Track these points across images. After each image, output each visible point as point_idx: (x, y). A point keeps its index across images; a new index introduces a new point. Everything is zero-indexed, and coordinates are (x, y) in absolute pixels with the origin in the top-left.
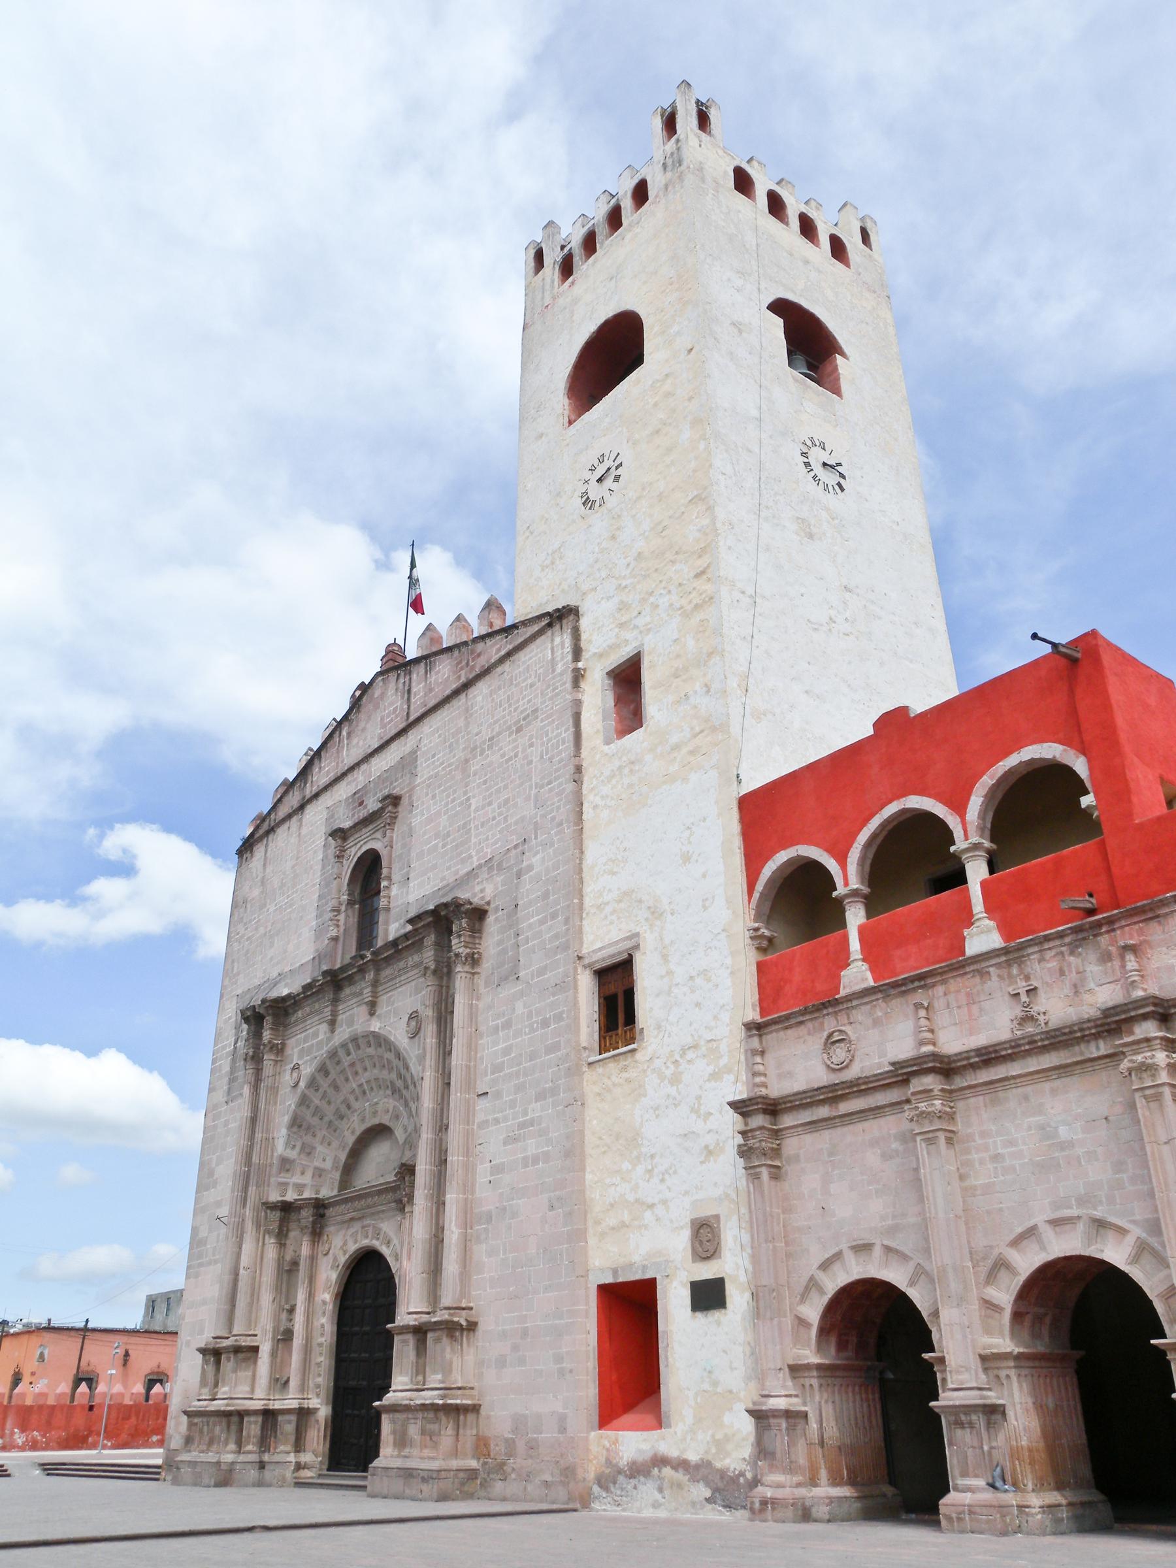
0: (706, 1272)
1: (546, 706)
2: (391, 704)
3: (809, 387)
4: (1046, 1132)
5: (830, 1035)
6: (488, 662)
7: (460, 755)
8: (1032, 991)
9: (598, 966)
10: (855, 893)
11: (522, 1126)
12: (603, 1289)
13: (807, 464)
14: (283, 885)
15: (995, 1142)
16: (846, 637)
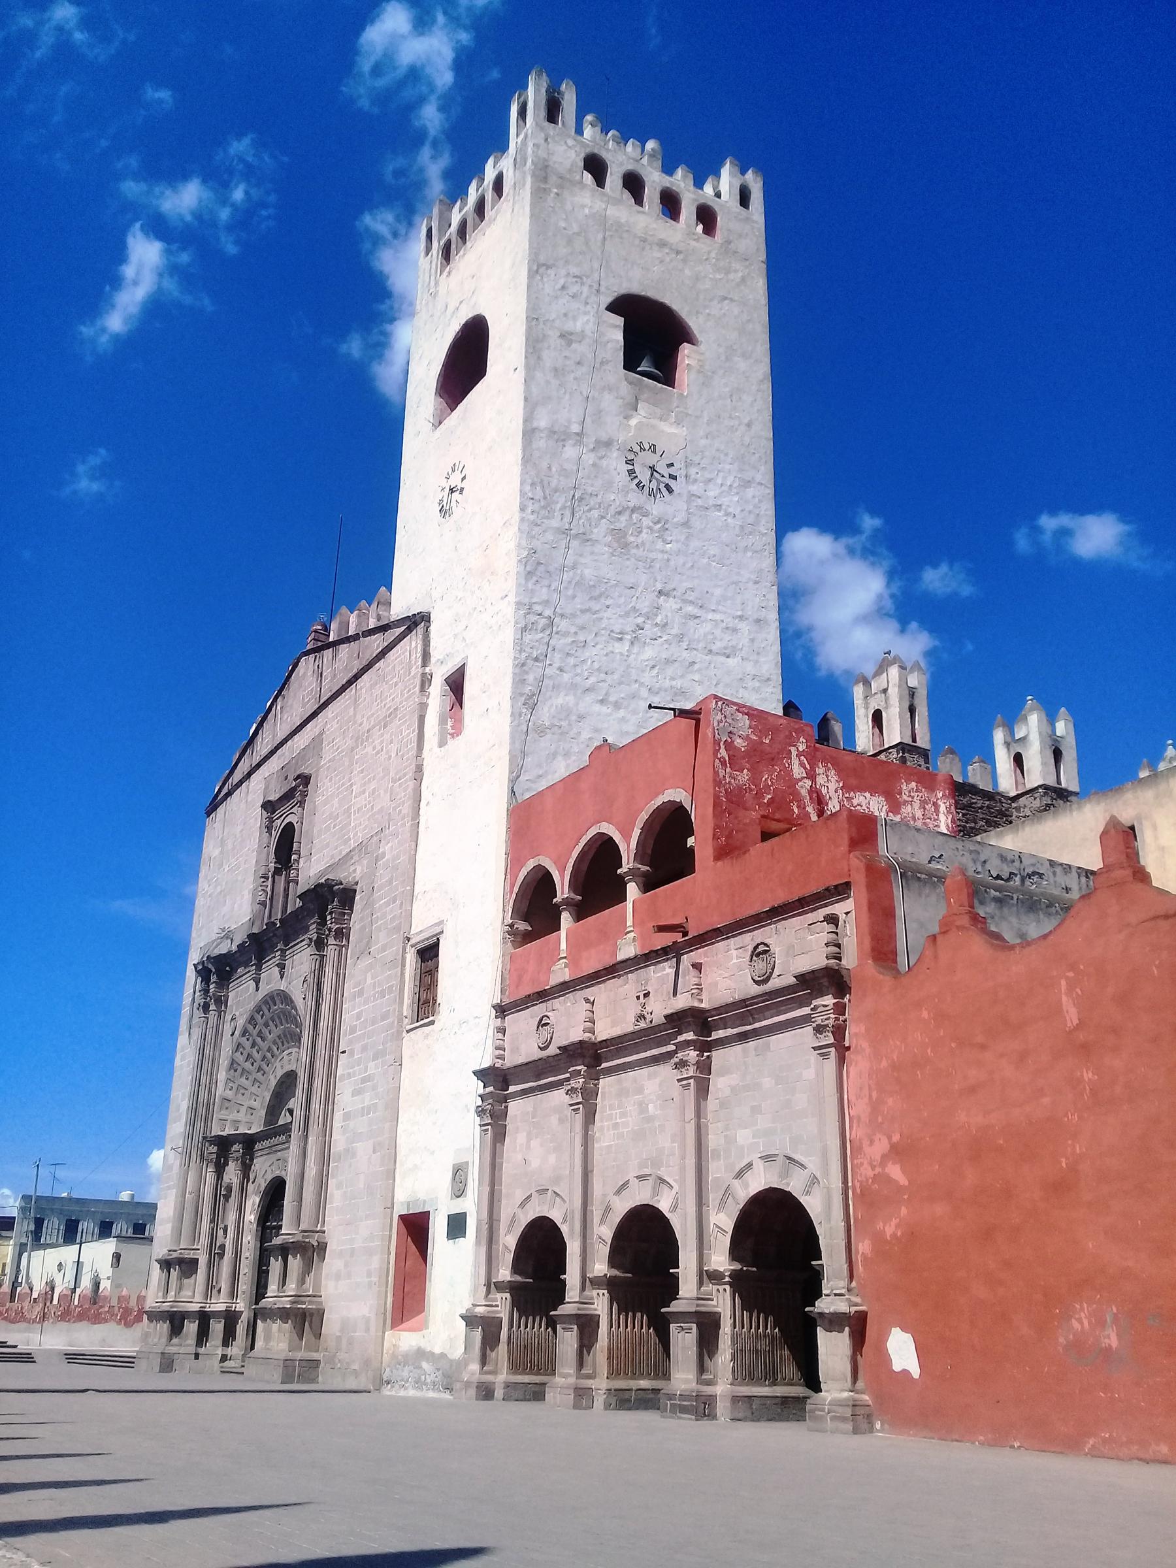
0: (457, 1207)
1: (403, 707)
3: (647, 386)
4: (642, 1107)
5: (541, 1020)
6: (371, 656)
7: (350, 742)
8: (647, 995)
9: (419, 946)
10: (567, 902)
11: (364, 1080)
12: (402, 1217)
13: (630, 472)
14: (233, 849)
16: (653, 642)
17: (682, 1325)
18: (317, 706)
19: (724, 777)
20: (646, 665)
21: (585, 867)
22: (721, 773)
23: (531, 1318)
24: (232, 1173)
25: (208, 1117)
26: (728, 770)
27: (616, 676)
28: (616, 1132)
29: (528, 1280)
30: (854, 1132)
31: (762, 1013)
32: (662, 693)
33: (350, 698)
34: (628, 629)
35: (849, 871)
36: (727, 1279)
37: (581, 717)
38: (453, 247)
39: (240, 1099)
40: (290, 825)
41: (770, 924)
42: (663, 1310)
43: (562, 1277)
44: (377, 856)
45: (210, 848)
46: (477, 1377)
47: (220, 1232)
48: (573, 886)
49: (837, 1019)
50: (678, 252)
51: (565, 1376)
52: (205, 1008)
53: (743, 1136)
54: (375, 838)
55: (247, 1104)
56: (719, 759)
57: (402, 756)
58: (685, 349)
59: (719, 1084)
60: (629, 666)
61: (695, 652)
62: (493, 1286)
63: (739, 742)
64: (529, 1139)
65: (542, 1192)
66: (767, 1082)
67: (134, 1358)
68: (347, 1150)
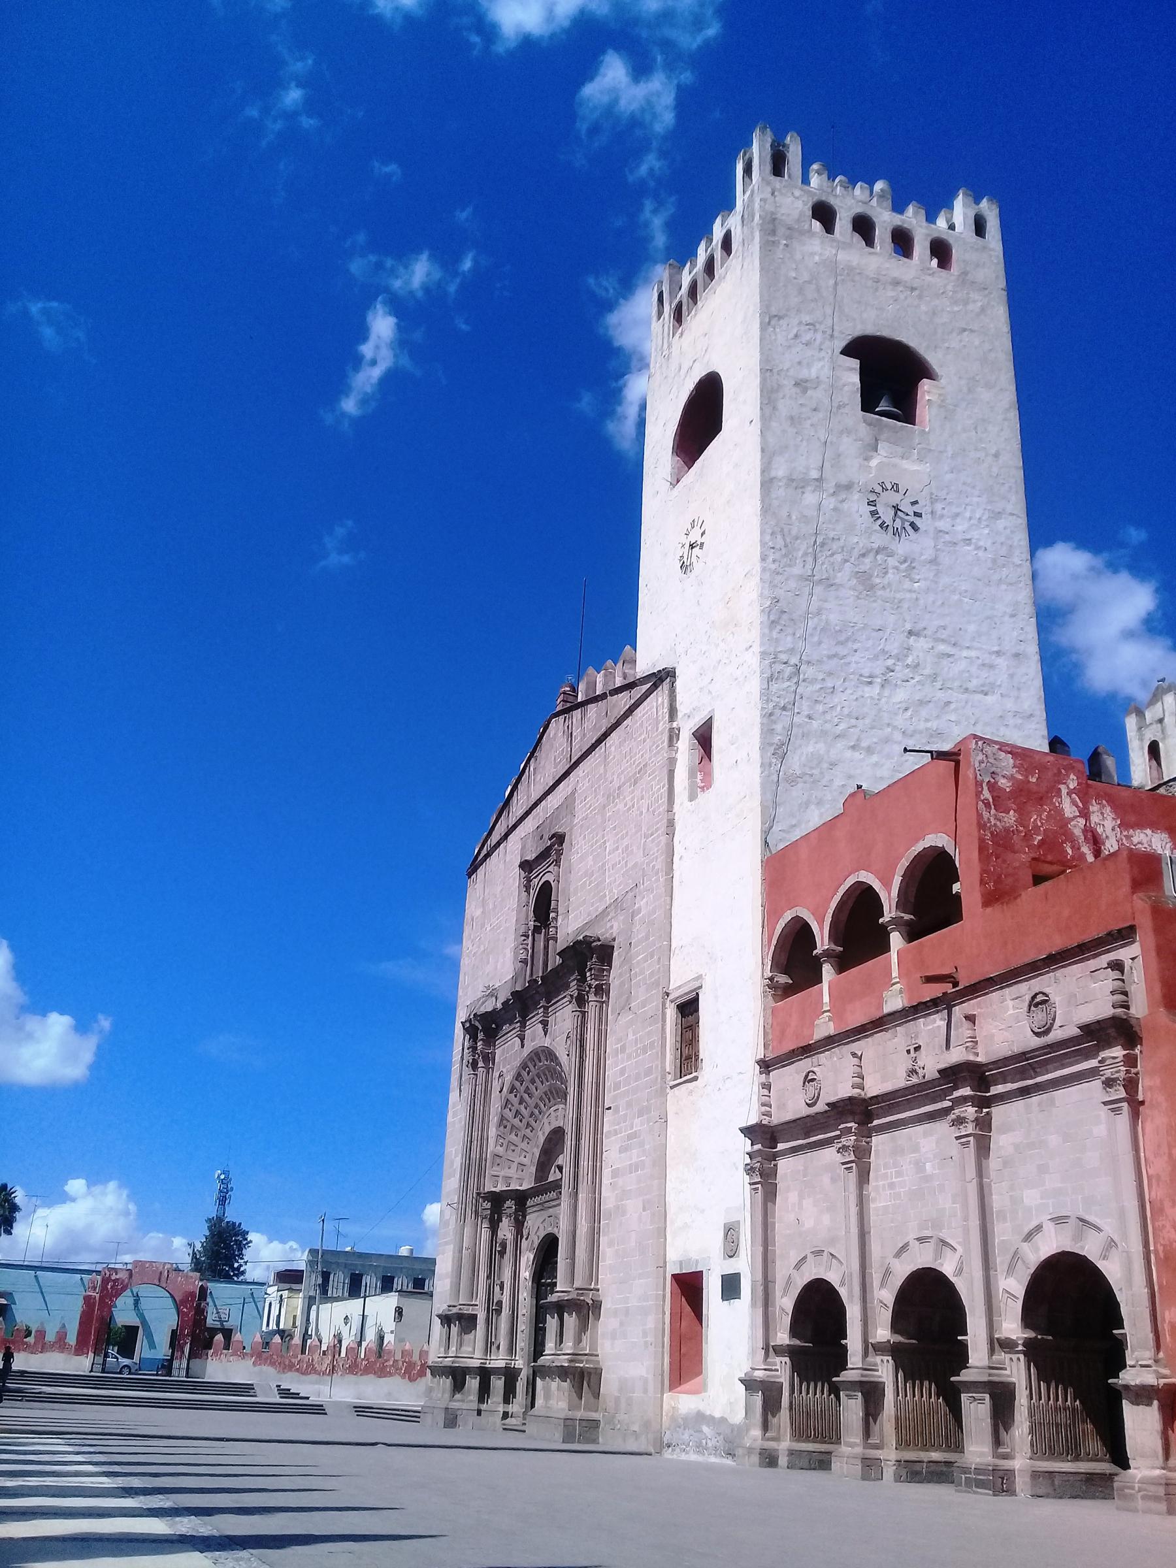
0: (730, 1267)
1: (652, 762)
2: (561, 745)
3: (886, 426)
4: (919, 1166)
5: (807, 1076)
7: (601, 800)
8: (917, 1049)
9: (679, 1001)
10: (827, 954)
11: (630, 1137)
12: (675, 1277)
13: (874, 513)
14: (495, 907)
15: (891, 1173)
17: (974, 1395)
18: (568, 766)
19: (989, 819)
20: (899, 708)
21: (844, 917)
22: (986, 815)
23: (812, 1385)
24: (506, 1230)
25: (481, 1174)
26: (993, 811)
27: (867, 721)
28: (892, 1192)
29: (807, 1344)
30: (1153, 1194)
31: (1044, 1066)
32: (918, 736)
33: (600, 756)
34: (878, 671)
35: (1134, 913)
36: (1020, 1348)
37: (833, 765)
38: (684, 308)
39: (510, 1154)
40: (547, 883)
41: (1048, 972)
42: (952, 1379)
43: (843, 1342)
44: (633, 912)
45: (472, 909)
46: (759, 1443)
47: (497, 1289)
48: (834, 936)
49: (1128, 1072)
50: (913, 289)
51: (852, 1445)
52: (474, 1065)
53: (1031, 1197)
54: (630, 894)
55: (517, 1160)
56: (983, 801)
57: (654, 811)
58: (925, 385)
59: (1001, 1142)
60: (880, 710)
61: (950, 691)
62: (771, 1349)
63: (1003, 783)
64: (801, 1197)
65: (819, 1253)
66: (1054, 1140)
67: (419, 1412)
68: (617, 1207)
